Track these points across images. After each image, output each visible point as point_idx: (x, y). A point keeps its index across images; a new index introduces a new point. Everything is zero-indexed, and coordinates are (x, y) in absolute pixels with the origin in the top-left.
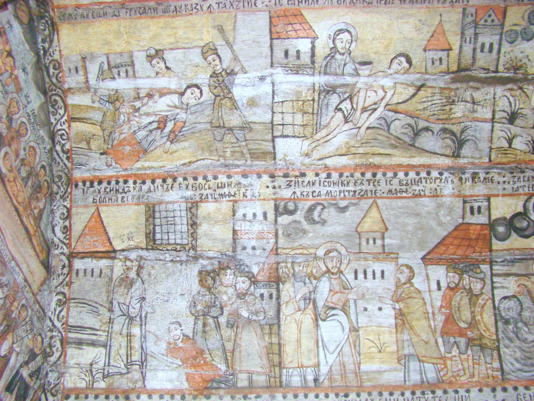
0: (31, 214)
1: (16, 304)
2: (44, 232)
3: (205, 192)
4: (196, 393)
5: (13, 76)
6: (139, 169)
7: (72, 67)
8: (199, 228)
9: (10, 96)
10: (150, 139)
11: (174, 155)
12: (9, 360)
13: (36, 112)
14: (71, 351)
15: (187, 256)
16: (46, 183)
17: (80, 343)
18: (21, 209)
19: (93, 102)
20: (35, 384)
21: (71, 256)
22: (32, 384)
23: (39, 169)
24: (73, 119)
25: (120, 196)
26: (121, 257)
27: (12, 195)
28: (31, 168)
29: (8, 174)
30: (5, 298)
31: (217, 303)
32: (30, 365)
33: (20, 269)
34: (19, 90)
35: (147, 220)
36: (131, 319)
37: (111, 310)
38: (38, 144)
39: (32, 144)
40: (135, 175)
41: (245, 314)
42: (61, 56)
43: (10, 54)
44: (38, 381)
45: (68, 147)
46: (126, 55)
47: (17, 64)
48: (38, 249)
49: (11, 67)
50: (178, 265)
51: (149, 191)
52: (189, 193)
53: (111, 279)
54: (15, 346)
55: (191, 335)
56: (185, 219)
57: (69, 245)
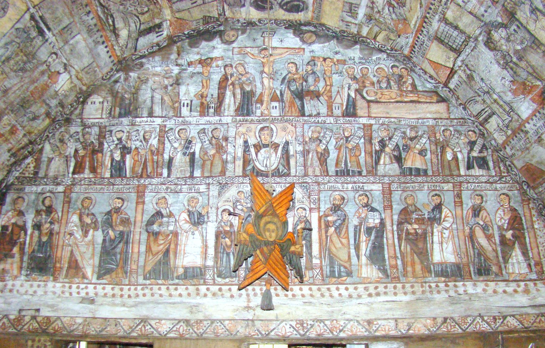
0: (407, 94)
1: (438, 135)
2: (424, 89)
3: (440, 10)
4: (541, 106)
5: (336, 63)
6: (414, 27)
7: (345, 26)
8: (459, 26)
9: (344, 70)
10: (398, 14)
11: (413, 8)
12: (457, 158)
13: (361, 56)
14: (487, 126)
15: (473, 42)
16: (403, 70)
17: (486, 120)
18: (399, 99)
19: (368, 27)
20: (488, 152)
21: (446, 85)
22: (485, 154)
23: (391, 71)
24: (375, 39)
25: (424, 45)
26: (457, 68)
27: (388, 101)
28: (386, 77)
29: (377, 97)
30: (429, 138)
31: (505, 53)
32: (475, 149)
33: (427, 119)
34: (344, 62)
35: (443, 45)
36: (488, 92)
37: (479, 96)
38: (379, 64)
39: (376, 68)
40: (417, 31)
41: (519, 48)
42: (338, 28)
43: (325, 60)
44: (489, 150)
45: (389, 48)
46: (345, 4)
47: (331, 57)
48: (428, 101)
49: (331, 62)
50: (475, 50)
51: (428, 32)
52: (437, 17)
53: (465, 81)
54: (455, 150)
55: (512, 79)
56: (451, 29)
57: (439, 82)
